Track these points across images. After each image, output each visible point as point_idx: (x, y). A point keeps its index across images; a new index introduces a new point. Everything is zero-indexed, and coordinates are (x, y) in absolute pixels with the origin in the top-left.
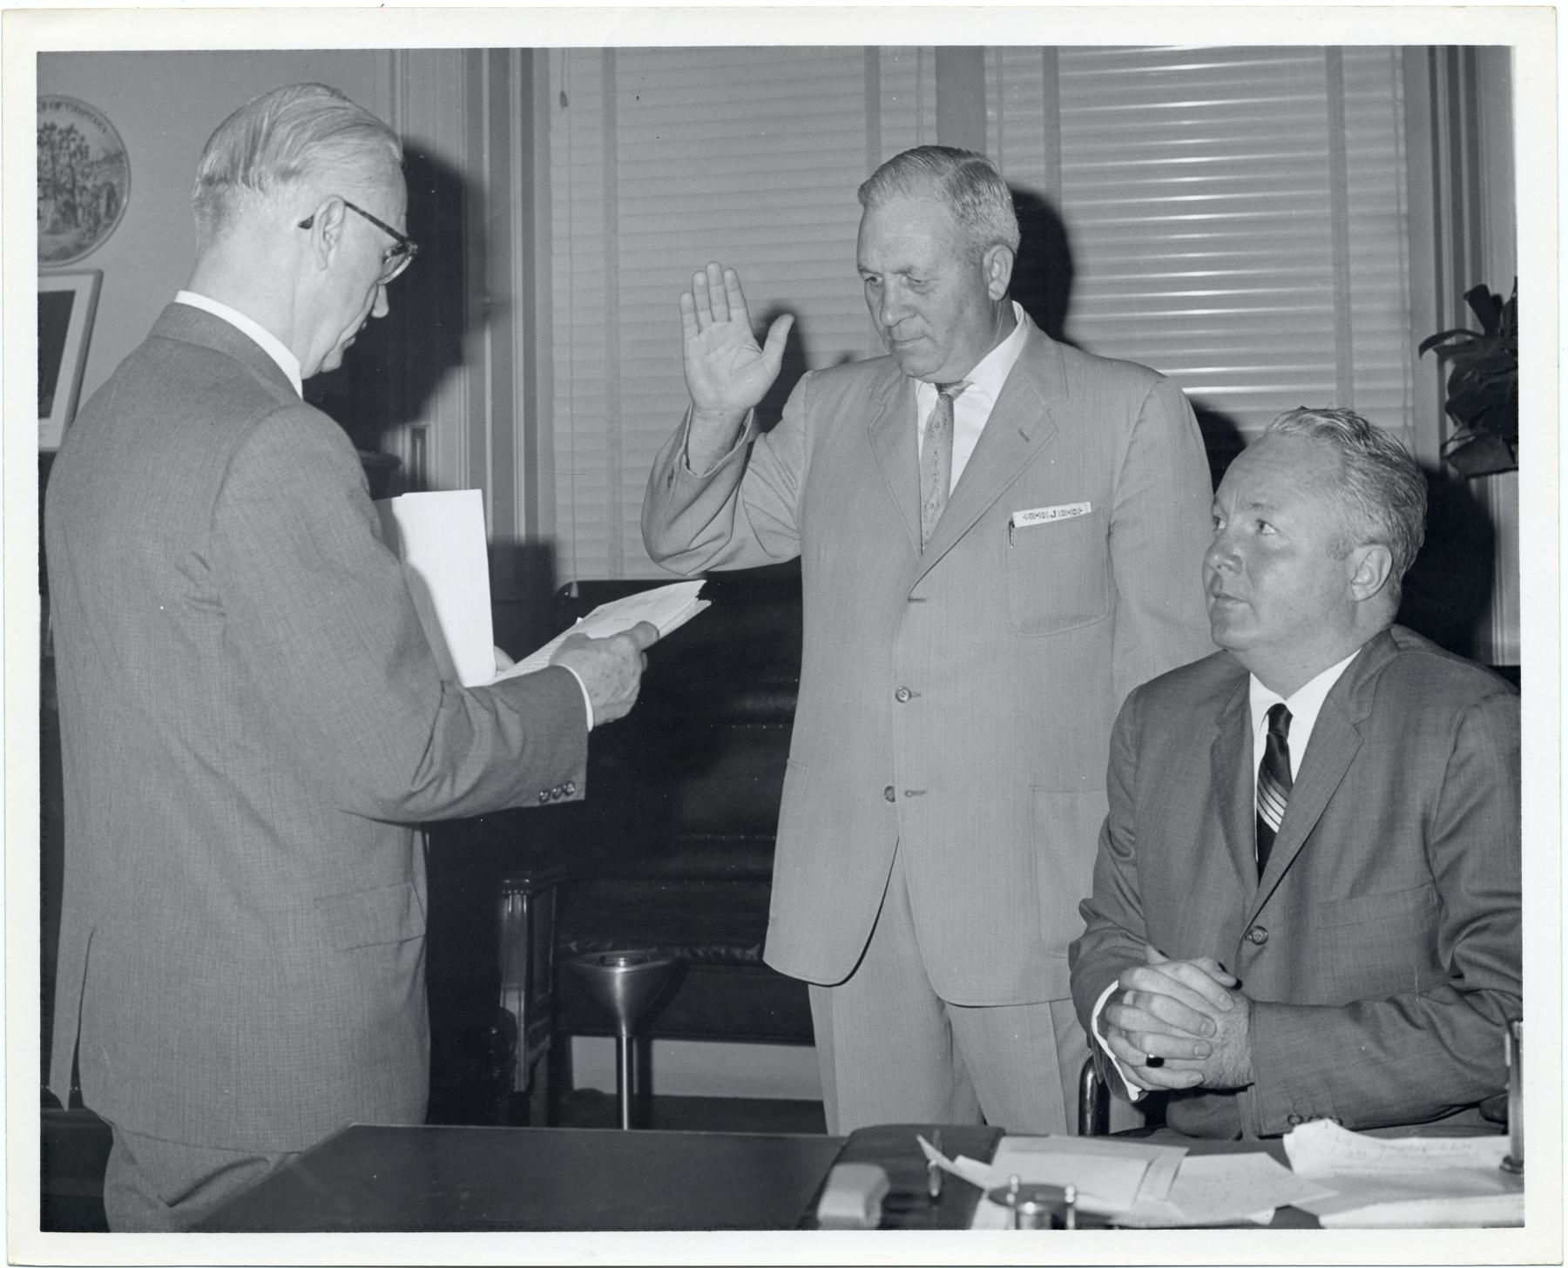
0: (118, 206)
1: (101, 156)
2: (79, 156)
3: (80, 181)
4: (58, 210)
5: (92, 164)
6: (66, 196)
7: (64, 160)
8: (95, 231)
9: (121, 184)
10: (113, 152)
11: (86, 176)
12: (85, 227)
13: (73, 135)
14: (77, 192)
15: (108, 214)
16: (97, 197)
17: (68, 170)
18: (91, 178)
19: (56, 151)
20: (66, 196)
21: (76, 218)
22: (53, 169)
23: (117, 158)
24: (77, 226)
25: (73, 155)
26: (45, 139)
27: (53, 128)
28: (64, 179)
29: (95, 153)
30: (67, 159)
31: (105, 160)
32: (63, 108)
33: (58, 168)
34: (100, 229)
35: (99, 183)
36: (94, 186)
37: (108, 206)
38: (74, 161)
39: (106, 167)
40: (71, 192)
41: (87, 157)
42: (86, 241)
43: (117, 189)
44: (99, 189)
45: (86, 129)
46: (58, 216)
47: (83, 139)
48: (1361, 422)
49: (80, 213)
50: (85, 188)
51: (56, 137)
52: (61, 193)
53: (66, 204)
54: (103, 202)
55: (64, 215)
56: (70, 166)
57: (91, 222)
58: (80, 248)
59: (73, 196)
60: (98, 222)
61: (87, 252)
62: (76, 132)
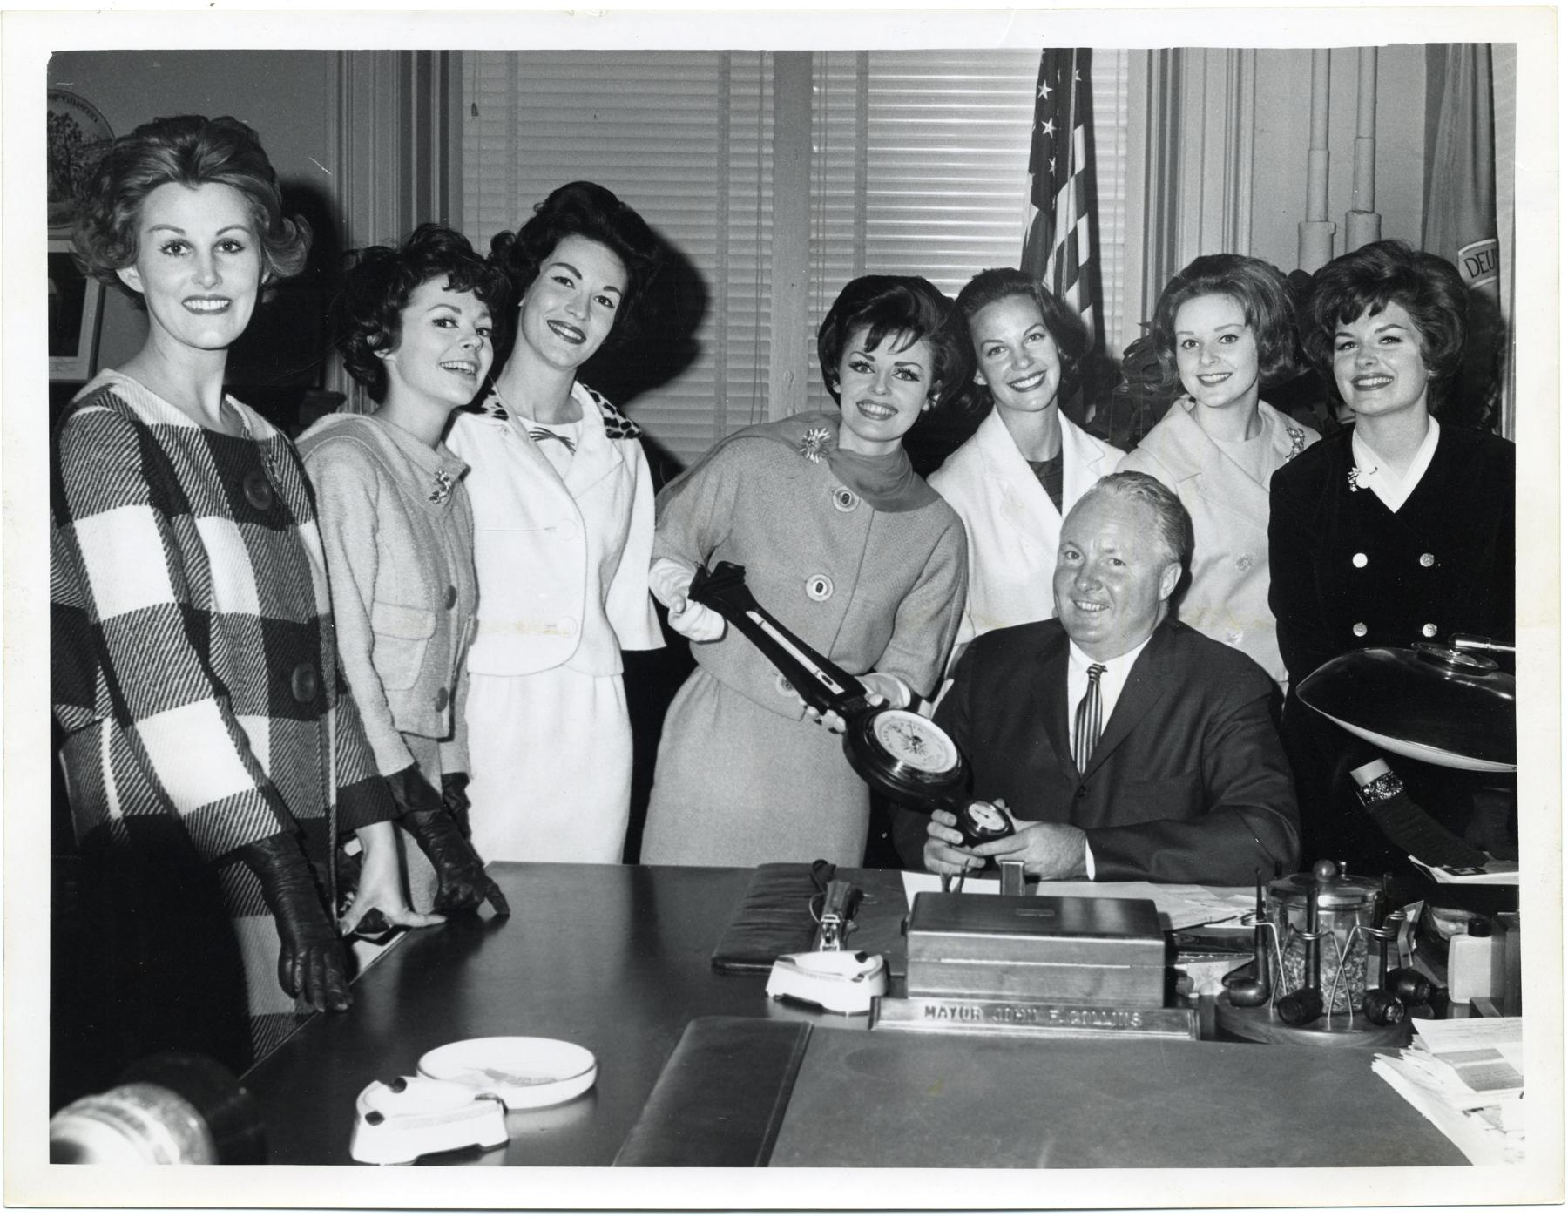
1: (93, 140)
5: (85, 146)
6: (62, 171)
11: (81, 156)
12: (79, 196)
13: (68, 122)
17: (64, 150)
18: (84, 158)
20: (62, 171)
21: (72, 190)
24: (73, 196)
28: (60, 157)
30: (63, 141)
31: (96, 144)
35: (91, 162)
36: (86, 164)
40: (67, 168)
47: (77, 125)
48: (1260, 275)
49: (74, 186)
53: (63, 177)
56: (65, 146)
59: (68, 171)
62: (71, 119)
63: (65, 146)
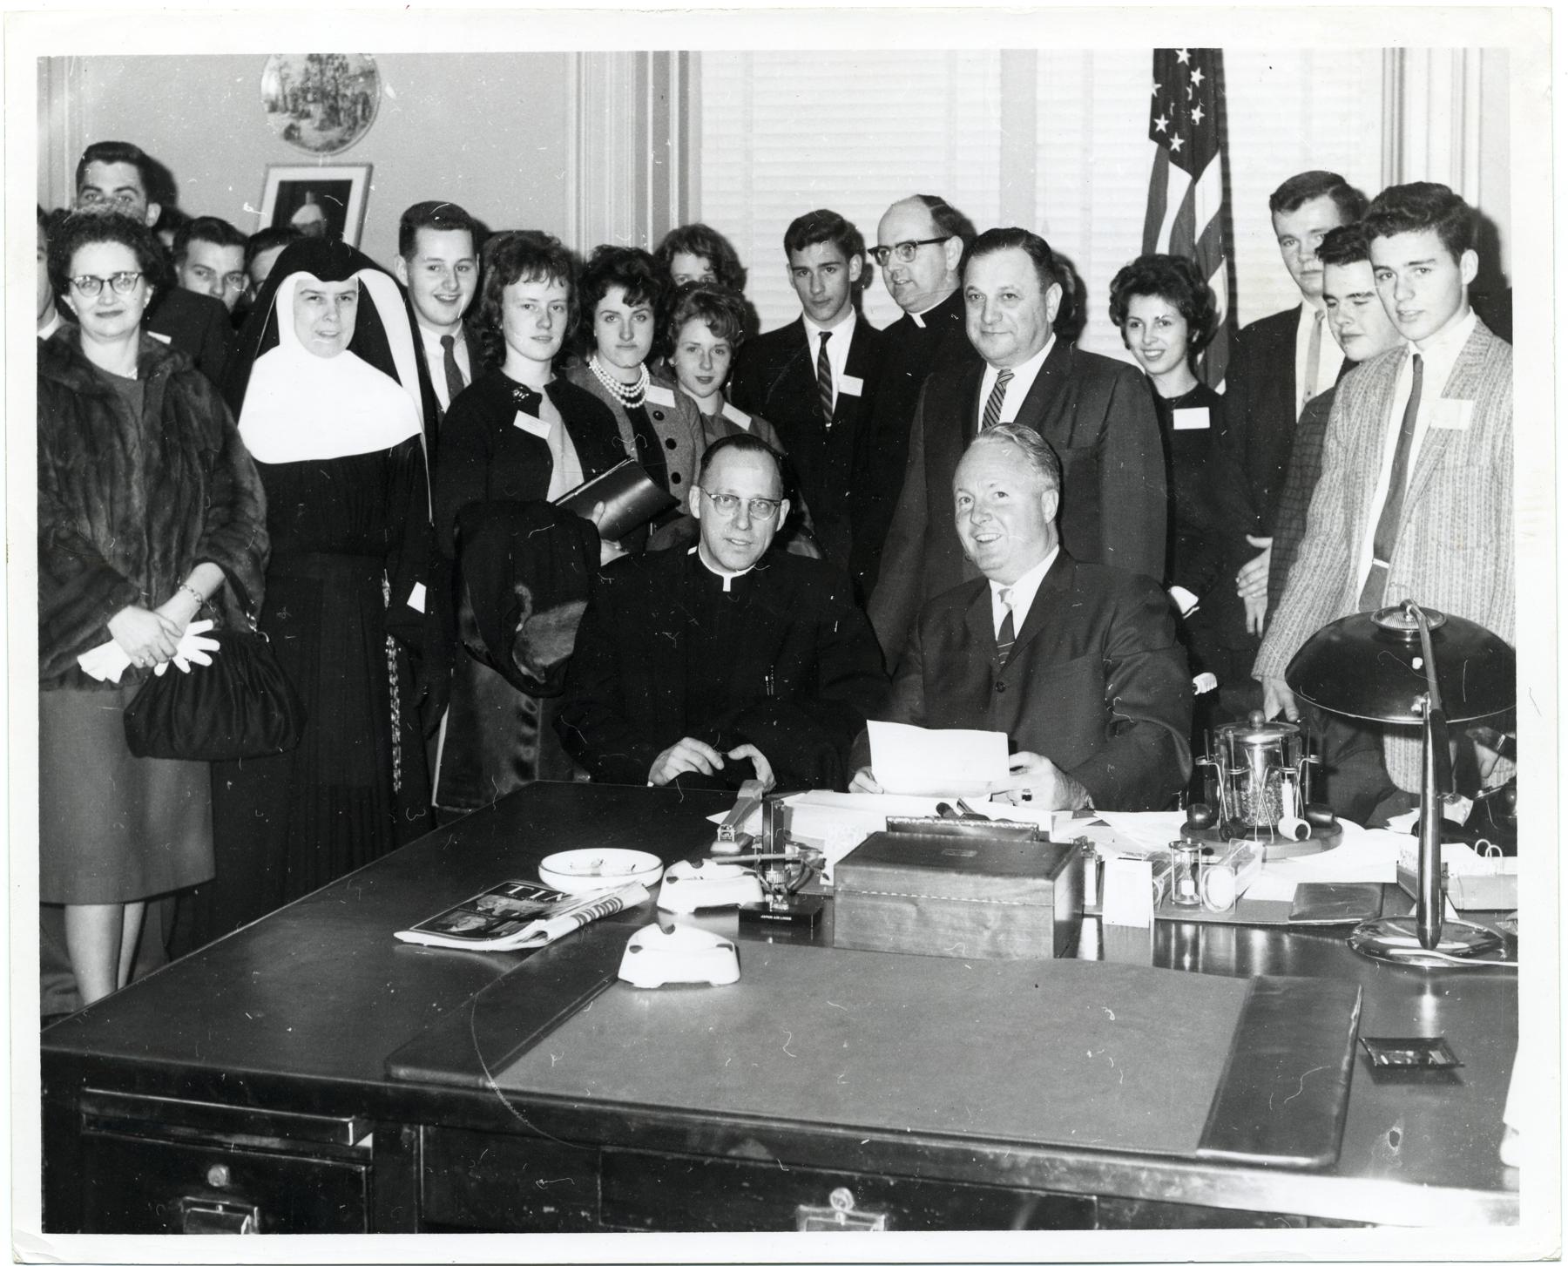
0: (370, 112)
1: (358, 72)
2: (341, 70)
7: (329, 73)
8: (354, 129)
9: (374, 93)
10: (367, 70)
11: (347, 86)
12: (346, 126)
16: (355, 103)
17: (333, 81)
19: (323, 67)
21: (339, 119)
24: (340, 124)
25: (337, 70)
28: (329, 88)
30: (332, 72)
33: (325, 79)
34: (357, 128)
35: (356, 92)
36: (353, 94)
37: (364, 111)
38: (337, 75)
40: (335, 98)
41: (347, 72)
42: (347, 137)
43: (370, 98)
44: (357, 96)
46: (324, 116)
49: (342, 115)
50: (345, 96)
52: (327, 98)
53: (331, 107)
54: (360, 107)
55: (329, 115)
56: (334, 78)
57: (351, 122)
58: (342, 142)
59: (336, 101)
60: (355, 122)
61: (348, 145)
63: (334, 78)
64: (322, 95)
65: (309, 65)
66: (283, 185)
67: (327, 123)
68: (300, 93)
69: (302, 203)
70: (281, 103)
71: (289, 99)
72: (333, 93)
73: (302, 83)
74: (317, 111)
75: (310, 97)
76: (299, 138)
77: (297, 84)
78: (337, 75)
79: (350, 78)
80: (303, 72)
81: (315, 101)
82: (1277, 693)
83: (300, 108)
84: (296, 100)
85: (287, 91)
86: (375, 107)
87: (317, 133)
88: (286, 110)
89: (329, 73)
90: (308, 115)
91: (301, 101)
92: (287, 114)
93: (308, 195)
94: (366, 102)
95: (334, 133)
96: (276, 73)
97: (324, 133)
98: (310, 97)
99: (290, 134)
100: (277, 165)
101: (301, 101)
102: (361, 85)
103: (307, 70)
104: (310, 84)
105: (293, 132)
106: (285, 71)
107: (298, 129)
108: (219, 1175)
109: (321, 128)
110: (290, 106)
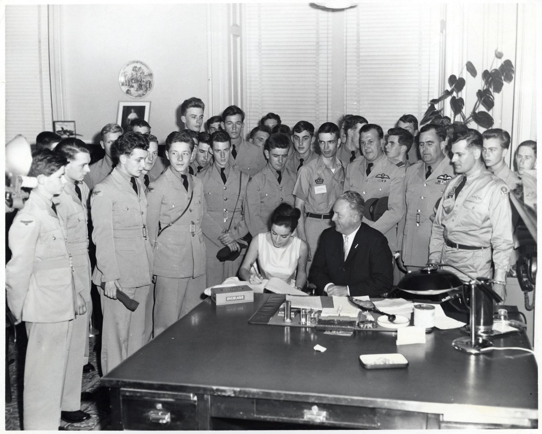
0: (151, 86)
1: (147, 74)
3: (143, 80)
4: (138, 86)
6: (140, 83)
7: (139, 74)
9: (152, 81)
12: (144, 90)
14: (142, 82)
15: (149, 87)
16: (147, 83)
19: (137, 72)
20: (140, 83)
22: (137, 76)
23: (151, 75)
24: (142, 89)
25: (141, 73)
26: (134, 69)
27: (136, 67)
29: (146, 73)
31: (148, 75)
32: (138, 63)
33: (138, 76)
34: (148, 91)
35: (147, 80)
37: (149, 86)
38: (141, 75)
39: (148, 77)
40: (141, 82)
42: (145, 93)
43: (151, 82)
45: (143, 67)
46: (137, 87)
47: (143, 70)
49: (143, 86)
50: (143, 81)
51: (137, 69)
53: (140, 84)
54: (148, 84)
55: (139, 87)
56: (140, 76)
57: (146, 89)
58: (143, 95)
59: (141, 82)
60: (147, 89)
61: (145, 96)
63: (140, 76)
64: (137, 81)
65: (133, 72)
66: (124, 107)
67: (139, 89)
68: (130, 80)
69: (131, 112)
70: (125, 83)
71: (127, 82)
72: (140, 80)
73: (131, 77)
74: (135, 85)
75: (133, 81)
76: (131, 93)
77: (130, 78)
78: (141, 75)
79: (145, 76)
80: (131, 74)
81: (135, 82)
82: (466, 278)
83: (131, 85)
84: (129, 83)
85: (126, 79)
86: (153, 85)
87: (136, 92)
88: (126, 85)
89: (139, 74)
90: (133, 87)
91: (131, 82)
92: (127, 86)
93: (132, 110)
94: (150, 83)
95: (141, 92)
96: (123, 74)
97: (138, 92)
98: (133, 81)
99: (128, 92)
100: (123, 101)
101: (131, 82)
102: (148, 79)
103: (132, 74)
104: (133, 77)
105: (129, 92)
106: (126, 74)
107: (130, 91)
108: (159, 406)
109: (137, 90)
110: (128, 84)
